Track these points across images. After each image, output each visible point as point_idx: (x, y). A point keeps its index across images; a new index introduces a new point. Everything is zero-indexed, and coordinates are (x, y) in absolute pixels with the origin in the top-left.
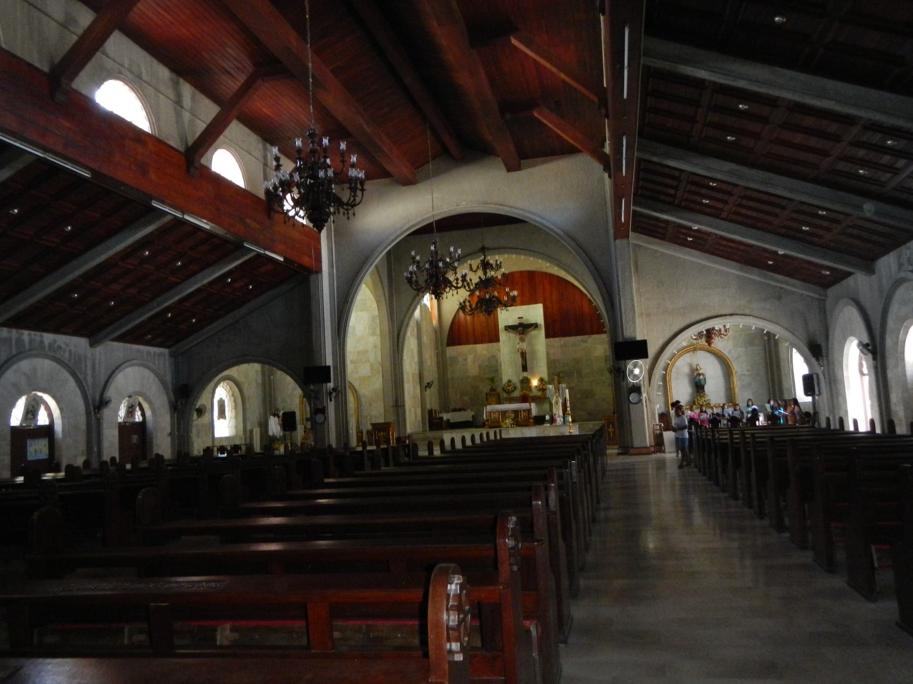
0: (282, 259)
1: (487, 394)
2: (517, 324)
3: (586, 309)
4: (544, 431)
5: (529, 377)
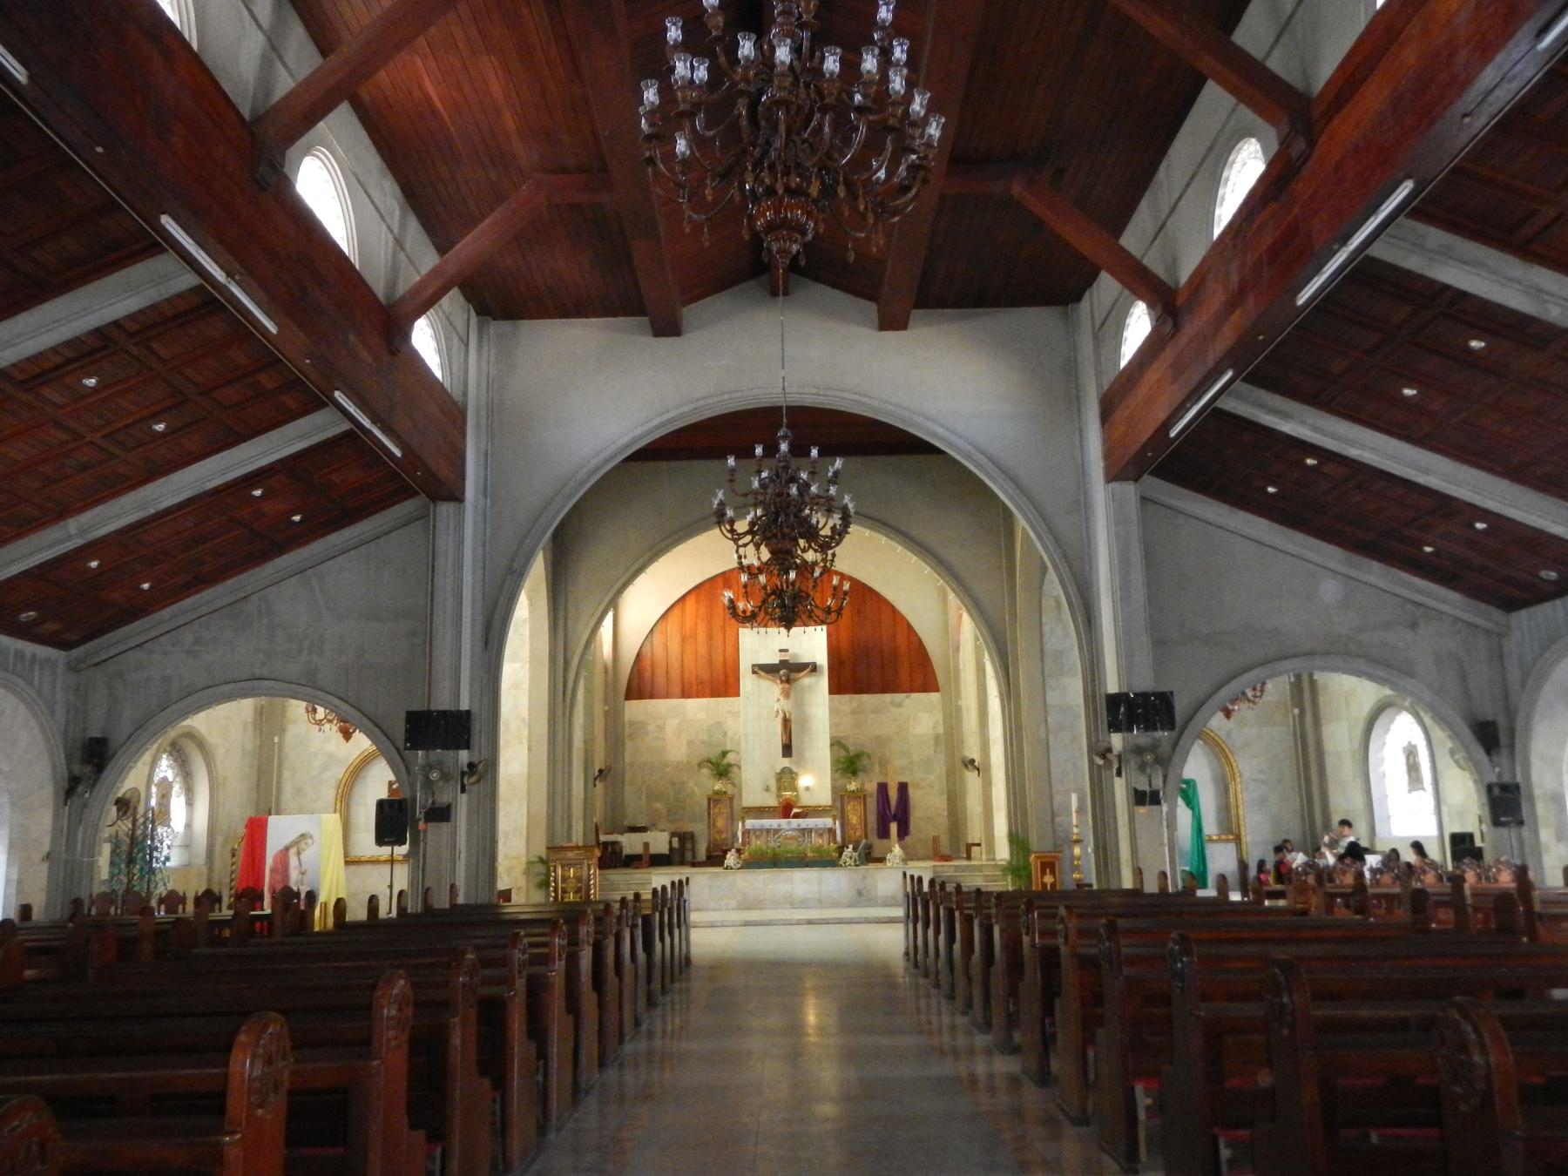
0: (398, 453)
1: (709, 800)
2: (777, 662)
3: (902, 641)
4: (864, 877)
5: (795, 769)
